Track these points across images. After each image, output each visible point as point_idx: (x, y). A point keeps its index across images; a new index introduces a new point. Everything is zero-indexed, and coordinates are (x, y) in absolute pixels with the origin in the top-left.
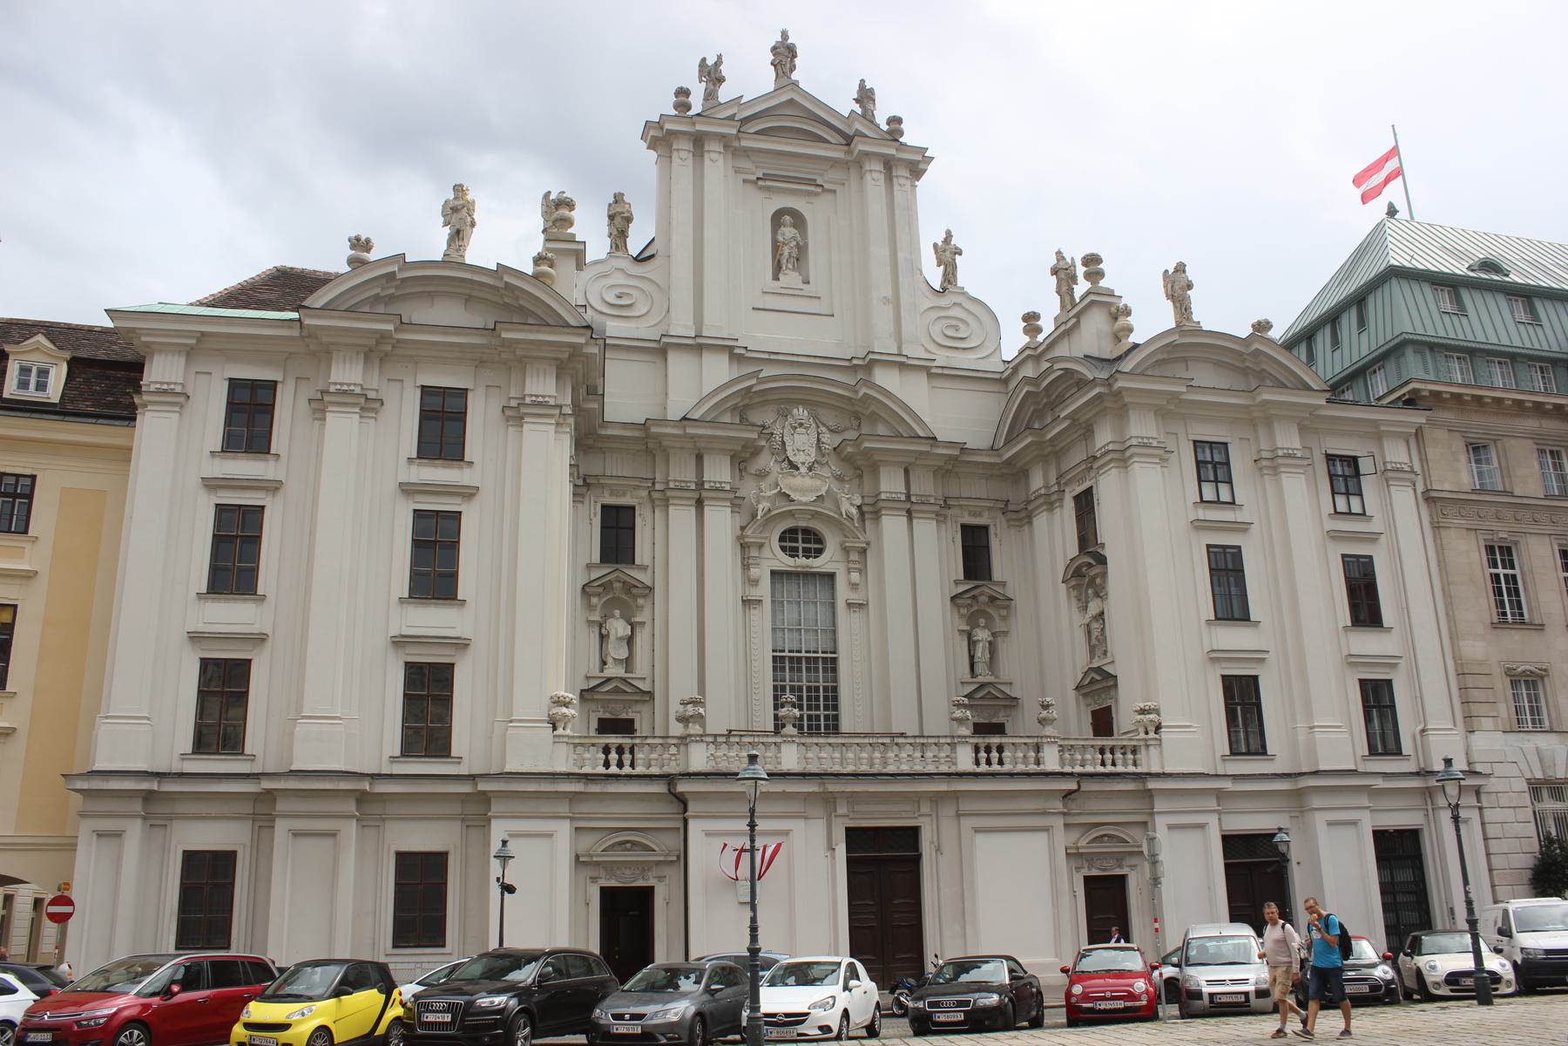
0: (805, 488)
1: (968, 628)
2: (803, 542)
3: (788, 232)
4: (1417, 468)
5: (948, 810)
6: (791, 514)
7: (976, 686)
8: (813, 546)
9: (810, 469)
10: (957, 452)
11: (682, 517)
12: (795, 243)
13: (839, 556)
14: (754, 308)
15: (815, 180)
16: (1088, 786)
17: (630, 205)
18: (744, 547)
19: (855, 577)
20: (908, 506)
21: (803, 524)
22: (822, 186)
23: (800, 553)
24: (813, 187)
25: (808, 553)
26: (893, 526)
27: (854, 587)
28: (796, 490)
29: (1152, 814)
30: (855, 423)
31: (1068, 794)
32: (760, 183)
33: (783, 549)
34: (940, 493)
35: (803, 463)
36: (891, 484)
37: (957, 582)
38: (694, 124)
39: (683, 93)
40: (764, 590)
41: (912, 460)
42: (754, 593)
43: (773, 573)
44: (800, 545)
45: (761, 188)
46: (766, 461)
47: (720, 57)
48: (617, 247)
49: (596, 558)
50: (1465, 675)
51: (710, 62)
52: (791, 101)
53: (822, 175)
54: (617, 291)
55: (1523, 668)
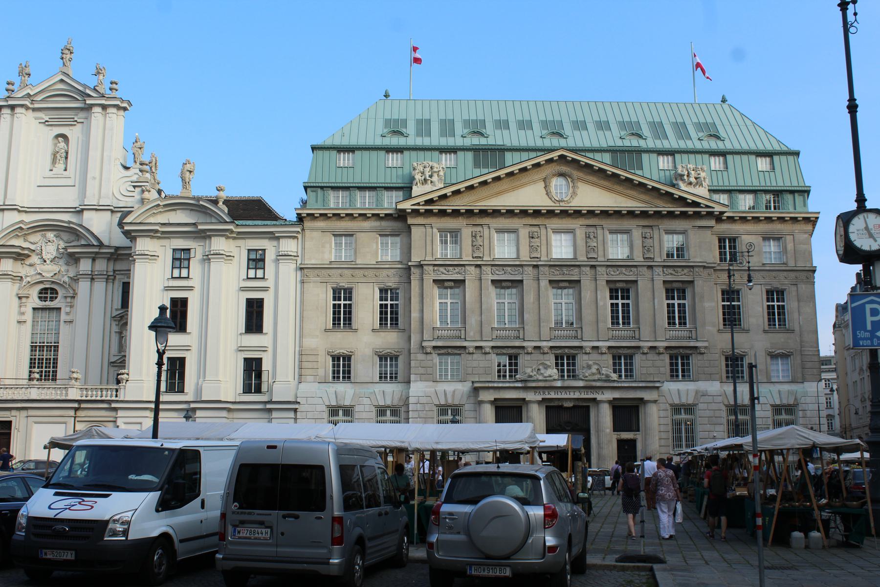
0: (49, 270)
1: (117, 330)
2: (51, 294)
3: (62, 145)
4: (299, 254)
5: (24, 413)
6: (41, 282)
7: (120, 357)
8: (54, 295)
9: (51, 261)
10: (112, 251)
12: (63, 151)
13: (63, 300)
14: (38, 186)
15: (74, 118)
16: (83, 406)
18: (20, 298)
19: (68, 309)
20: (91, 276)
21: (47, 286)
22: (76, 121)
23: (49, 299)
24: (72, 123)
25: (52, 299)
26: (83, 286)
27: (68, 314)
28: (45, 272)
29: (116, 418)
30: (77, 238)
31: (76, 409)
32: (47, 123)
33: (40, 298)
34: (111, 269)
36: (85, 266)
37: (117, 310)
38: (7, 101)
40: (29, 316)
41: (94, 256)
42: (23, 318)
43: (34, 309)
44: (49, 295)
46: (34, 259)
50: (302, 356)
52: (62, 81)
53: (77, 115)
55: (338, 351)
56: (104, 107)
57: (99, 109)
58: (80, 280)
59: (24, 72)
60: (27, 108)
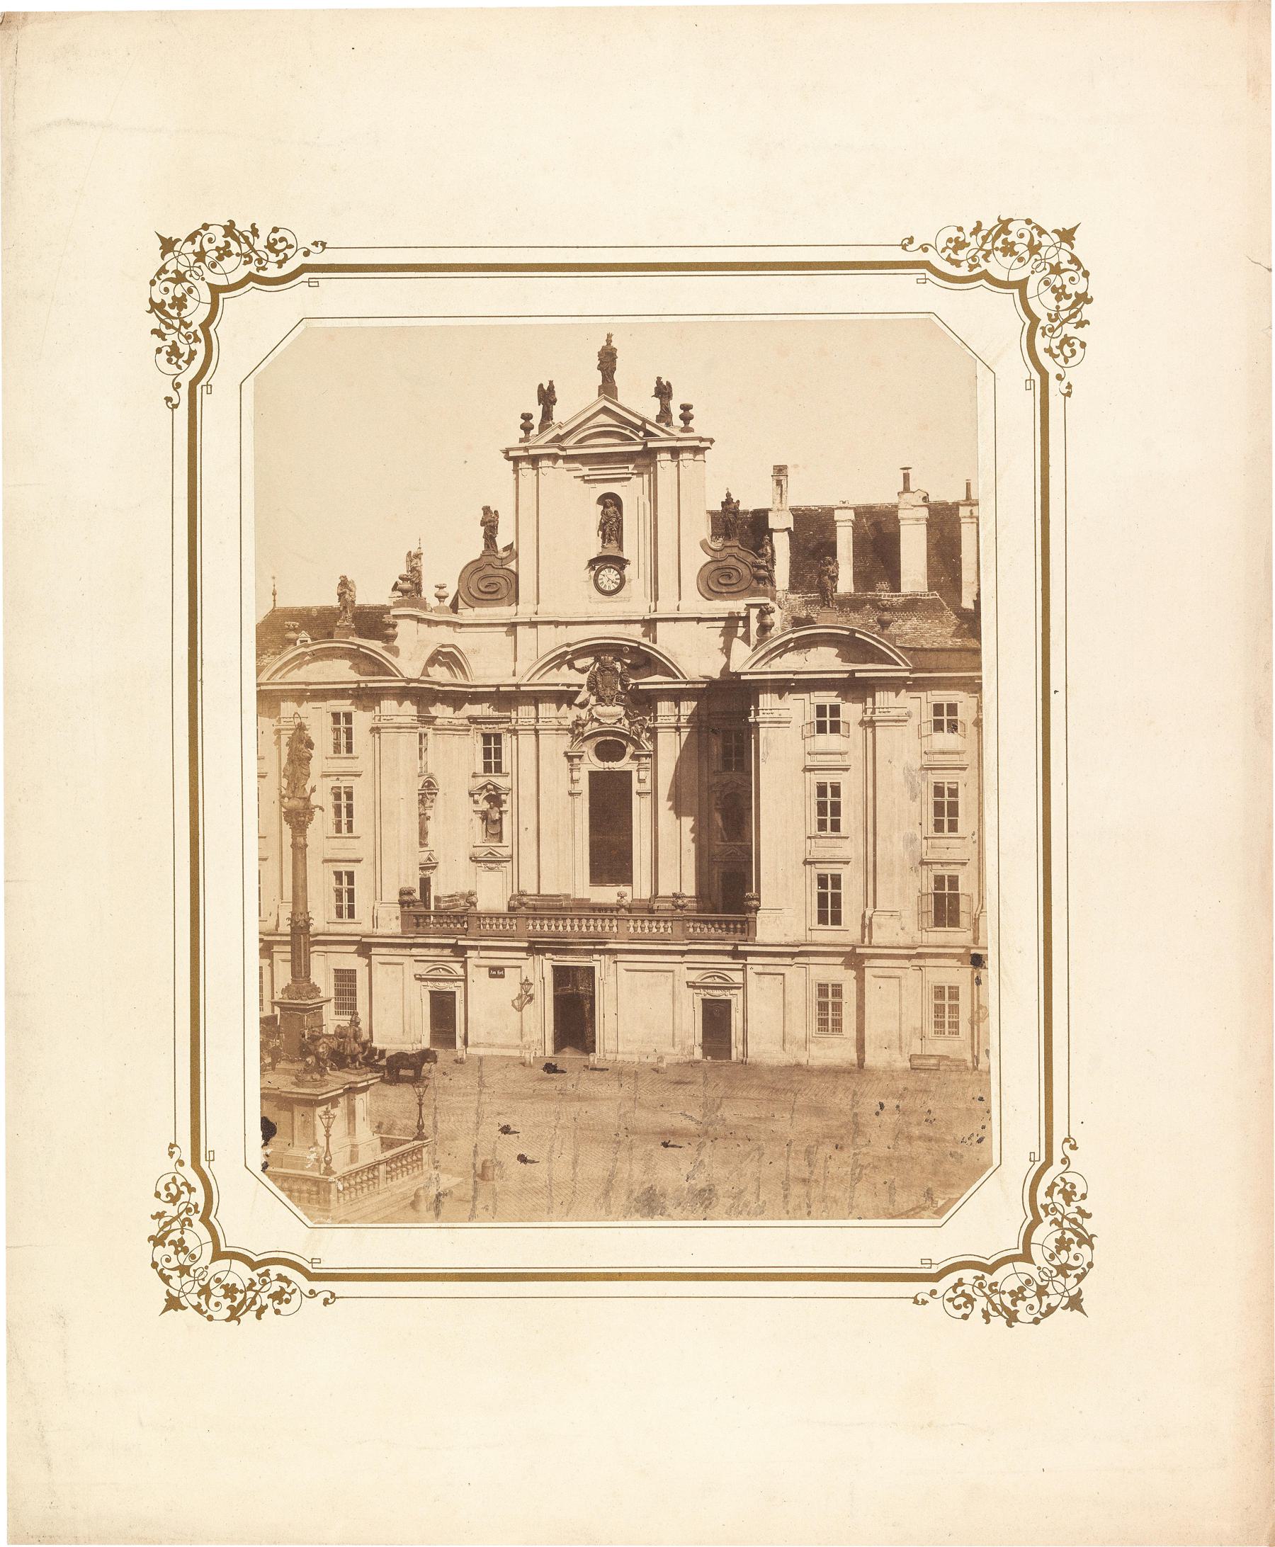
11: (527, 741)
17: (496, 512)
18: (570, 758)
35: (608, 697)
39: (526, 417)
42: (577, 788)
45: (586, 481)
47: (551, 382)
48: (488, 547)
49: (480, 768)
51: (546, 388)
54: (486, 582)
56: (675, 452)
57: (668, 456)
58: (659, 730)
59: (547, 397)
60: (554, 457)
